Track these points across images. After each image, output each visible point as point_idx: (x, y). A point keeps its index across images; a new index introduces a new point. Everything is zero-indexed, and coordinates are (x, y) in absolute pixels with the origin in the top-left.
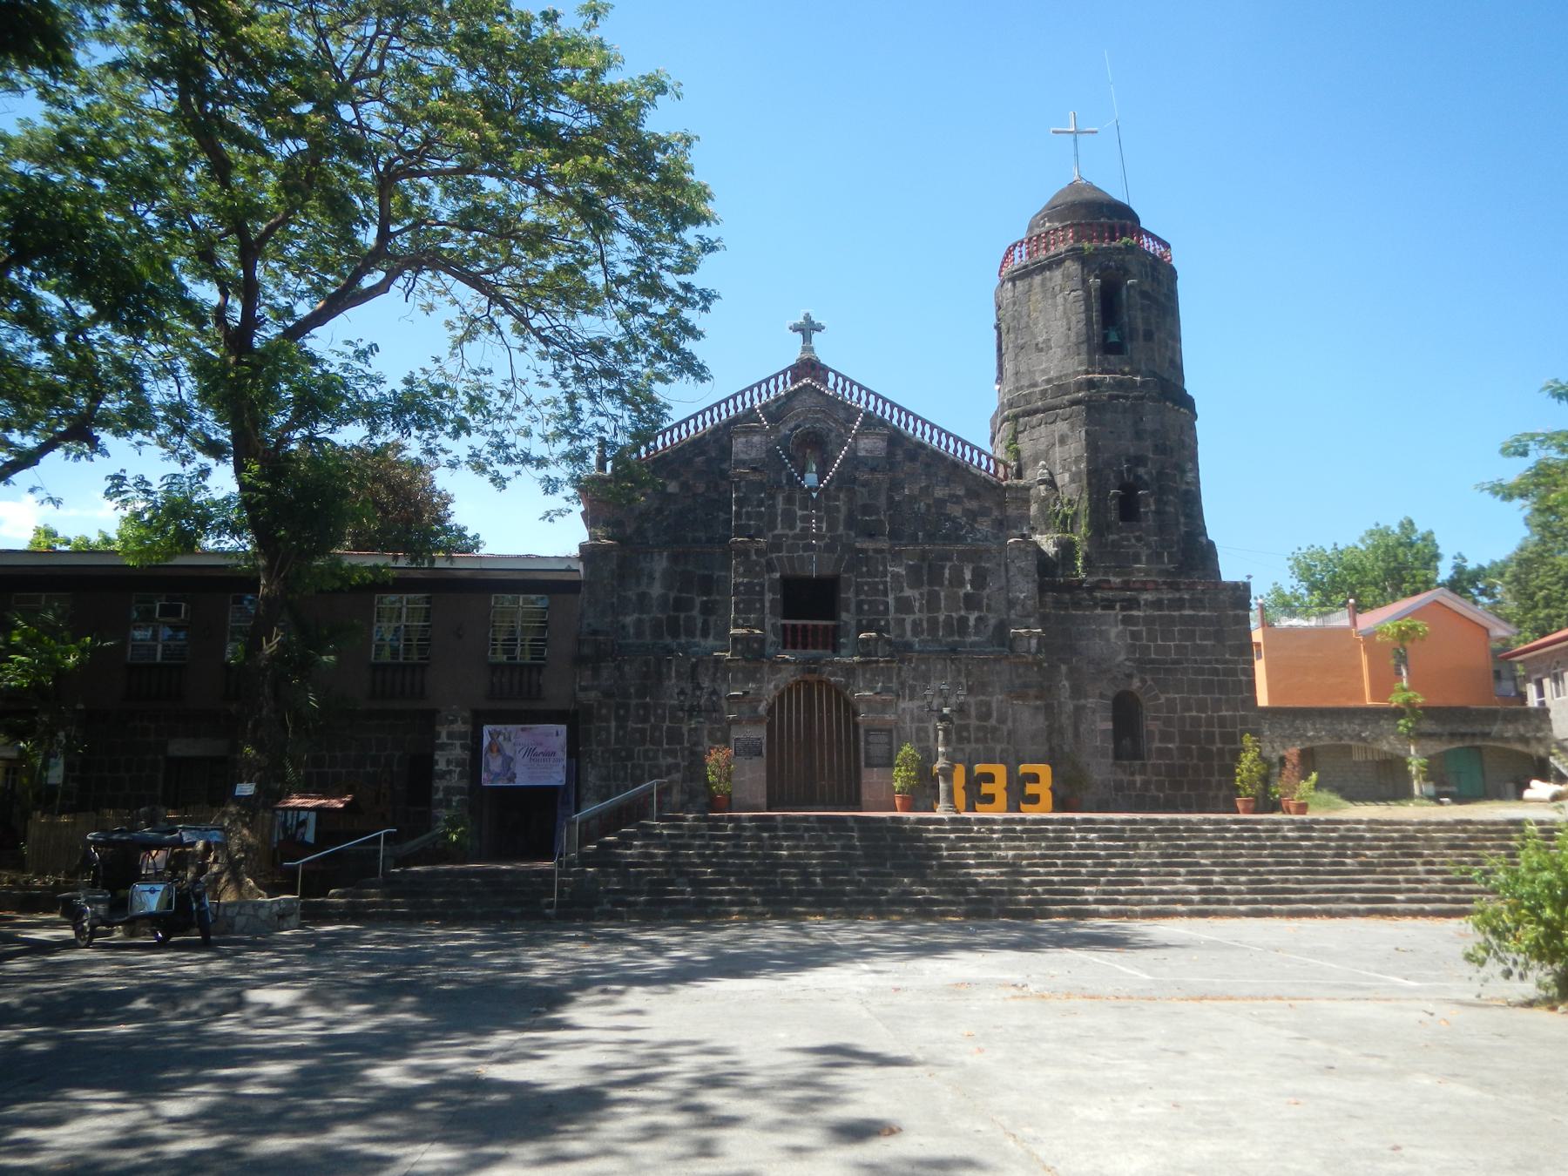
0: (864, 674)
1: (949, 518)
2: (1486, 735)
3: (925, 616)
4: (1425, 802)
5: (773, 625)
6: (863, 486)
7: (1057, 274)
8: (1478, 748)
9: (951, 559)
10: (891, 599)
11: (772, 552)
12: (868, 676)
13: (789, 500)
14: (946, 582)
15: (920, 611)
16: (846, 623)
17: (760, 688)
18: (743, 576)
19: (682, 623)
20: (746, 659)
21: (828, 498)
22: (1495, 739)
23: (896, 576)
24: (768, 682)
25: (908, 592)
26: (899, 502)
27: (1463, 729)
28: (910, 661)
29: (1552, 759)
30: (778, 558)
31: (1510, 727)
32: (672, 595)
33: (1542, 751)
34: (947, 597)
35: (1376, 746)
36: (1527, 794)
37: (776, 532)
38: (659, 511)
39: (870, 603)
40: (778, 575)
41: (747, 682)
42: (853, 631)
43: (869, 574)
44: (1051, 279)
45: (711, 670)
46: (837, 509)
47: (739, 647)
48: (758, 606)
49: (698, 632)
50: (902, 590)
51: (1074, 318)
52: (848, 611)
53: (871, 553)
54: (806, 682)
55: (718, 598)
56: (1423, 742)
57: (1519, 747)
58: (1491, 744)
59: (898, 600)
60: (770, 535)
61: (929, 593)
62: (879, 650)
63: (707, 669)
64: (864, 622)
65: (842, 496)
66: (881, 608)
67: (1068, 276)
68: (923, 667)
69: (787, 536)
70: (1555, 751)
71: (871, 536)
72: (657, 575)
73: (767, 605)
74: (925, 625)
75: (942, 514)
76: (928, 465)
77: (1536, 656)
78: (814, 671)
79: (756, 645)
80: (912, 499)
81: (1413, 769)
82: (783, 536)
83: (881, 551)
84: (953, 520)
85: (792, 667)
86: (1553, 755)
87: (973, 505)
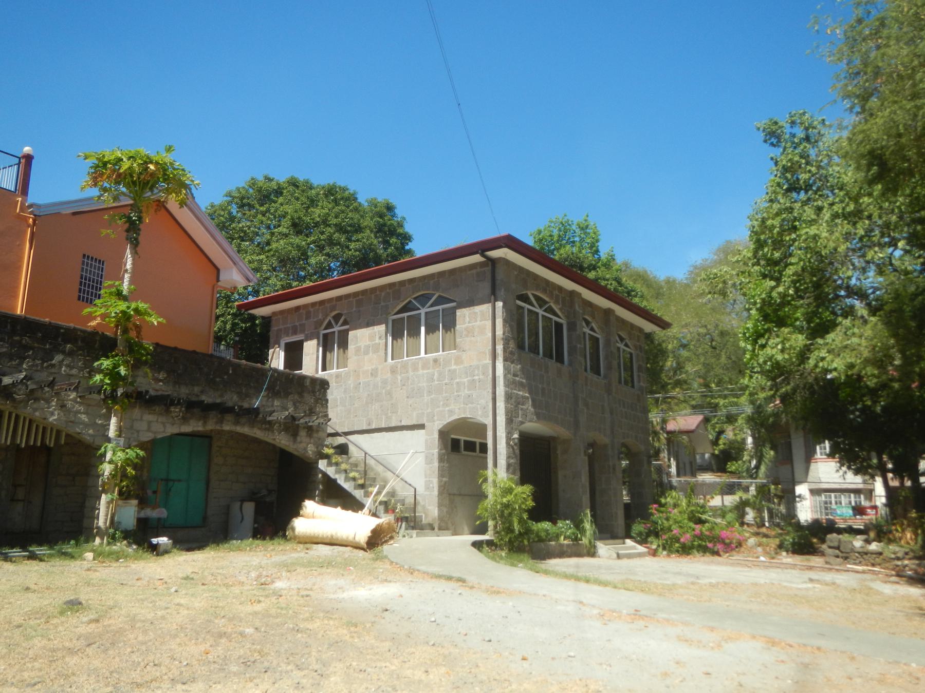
2: (252, 415)
4: (120, 546)
8: (206, 437)
22: (252, 424)
27: (207, 399)
29: (322, 465)
31: (277, 403)
33: (311, 450)
35: (30, 411)
36: (300, 525)
56: (136, 412)
57: (282, 440)
58: (245, 430)
70: (330, 451)
77: (298, 308)
81: (107, 469)
86: (327, 457)
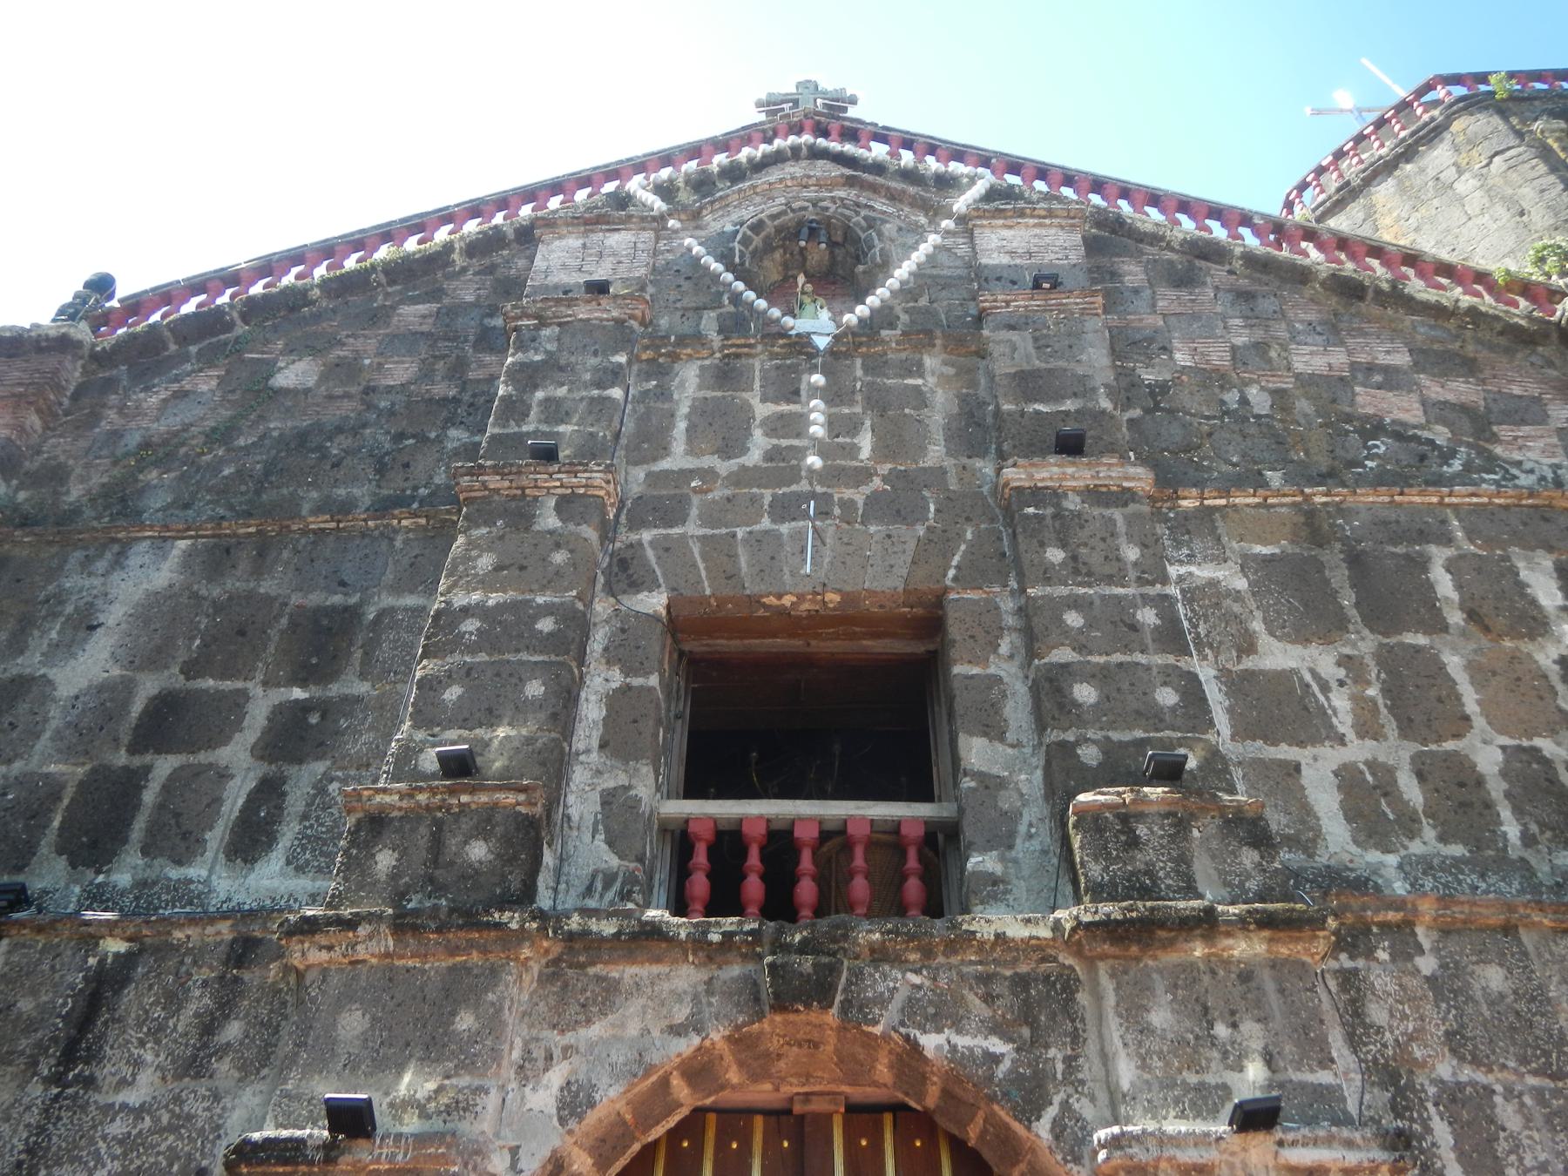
0: (1133, 1012)
1: (1375, 428)
3: (1397, 752)
5: (608, 798)
6: (1012, 327)
7: (1439, 157)
9: (1447, 540)
10: (1206, 673)
11: (636, 523)
12: (1160, 1017)
13: (727, 374)
14: (1456, 618)
15: (1367, 728)
16: (991, 784)
17: (461, 1107)
18: (486, 583)
19: (149, 796)
20: (404, 925)
21: (875, 366)
23: (1206, 596)
24: (527, 1072)
25: (1276, 655)
26: (1163, 387)
28: (1402, 935)
30: (665, 548)
32: (149, 686)
34: (1476, 671)
37: (665, 464)
38: (221, 435)
39: (1101, 676)
40: (655, 602)
41: (386, 1062)
42: (1034, 814)
43: (1077, 568)
44: (1422, 170)
45: (199, 1001)
46: (920, 399)
47: (385, 860)
48: (534, 689)
49: (216, 837)
50: (1247, 646)
51: (1527, 194)
52: (994, 730)
53: (1073, 503)
54: (780, 1117)
55: (362, 688)
59: (1239, 685)
60: (639, 473)
61: (1386, 657)
62: (1202, 868)
63: (174, 1000)
64: (1090, 755)
65: (929, 362)
66: (1167, 697)
67: (1469, 141)
68: (1494, 978)
69: (708, 475)
71: (1071, 446)
72: (114, 616)
73: (591, 710)
74: (1412, 791)
75: (1349, 418)
76: (1245, 297)
78: (819, 990)
79: (478, 851)
80: (1212, 379)
82: (688, 474)
83: (1125, 497)
84: (1400, 434)
85: (686, 976)
87: (1460, 390)
